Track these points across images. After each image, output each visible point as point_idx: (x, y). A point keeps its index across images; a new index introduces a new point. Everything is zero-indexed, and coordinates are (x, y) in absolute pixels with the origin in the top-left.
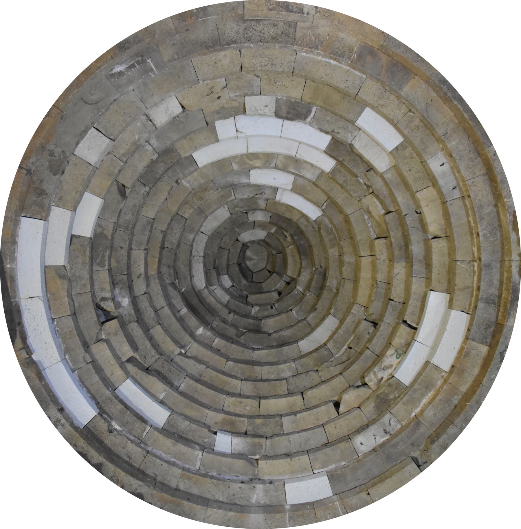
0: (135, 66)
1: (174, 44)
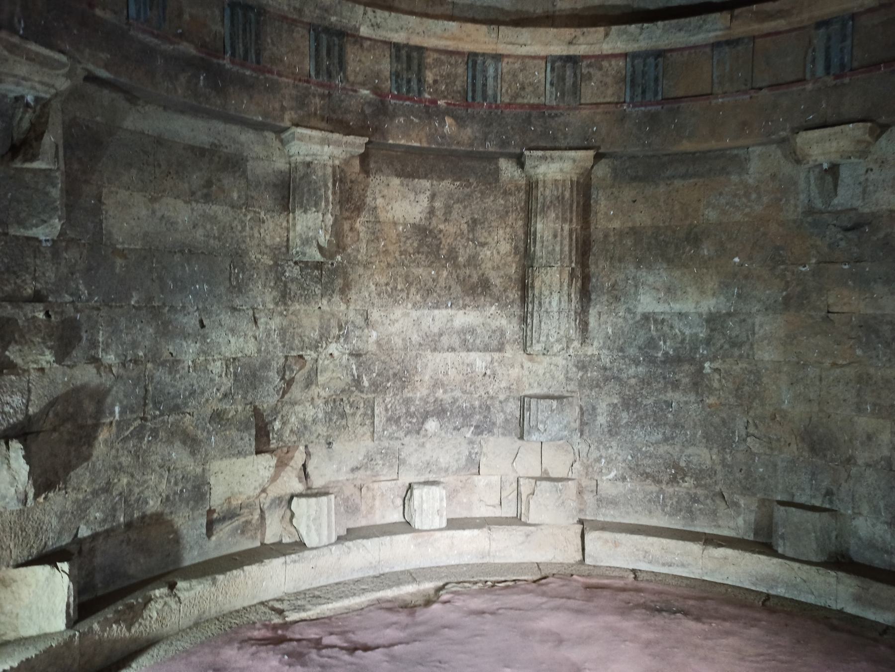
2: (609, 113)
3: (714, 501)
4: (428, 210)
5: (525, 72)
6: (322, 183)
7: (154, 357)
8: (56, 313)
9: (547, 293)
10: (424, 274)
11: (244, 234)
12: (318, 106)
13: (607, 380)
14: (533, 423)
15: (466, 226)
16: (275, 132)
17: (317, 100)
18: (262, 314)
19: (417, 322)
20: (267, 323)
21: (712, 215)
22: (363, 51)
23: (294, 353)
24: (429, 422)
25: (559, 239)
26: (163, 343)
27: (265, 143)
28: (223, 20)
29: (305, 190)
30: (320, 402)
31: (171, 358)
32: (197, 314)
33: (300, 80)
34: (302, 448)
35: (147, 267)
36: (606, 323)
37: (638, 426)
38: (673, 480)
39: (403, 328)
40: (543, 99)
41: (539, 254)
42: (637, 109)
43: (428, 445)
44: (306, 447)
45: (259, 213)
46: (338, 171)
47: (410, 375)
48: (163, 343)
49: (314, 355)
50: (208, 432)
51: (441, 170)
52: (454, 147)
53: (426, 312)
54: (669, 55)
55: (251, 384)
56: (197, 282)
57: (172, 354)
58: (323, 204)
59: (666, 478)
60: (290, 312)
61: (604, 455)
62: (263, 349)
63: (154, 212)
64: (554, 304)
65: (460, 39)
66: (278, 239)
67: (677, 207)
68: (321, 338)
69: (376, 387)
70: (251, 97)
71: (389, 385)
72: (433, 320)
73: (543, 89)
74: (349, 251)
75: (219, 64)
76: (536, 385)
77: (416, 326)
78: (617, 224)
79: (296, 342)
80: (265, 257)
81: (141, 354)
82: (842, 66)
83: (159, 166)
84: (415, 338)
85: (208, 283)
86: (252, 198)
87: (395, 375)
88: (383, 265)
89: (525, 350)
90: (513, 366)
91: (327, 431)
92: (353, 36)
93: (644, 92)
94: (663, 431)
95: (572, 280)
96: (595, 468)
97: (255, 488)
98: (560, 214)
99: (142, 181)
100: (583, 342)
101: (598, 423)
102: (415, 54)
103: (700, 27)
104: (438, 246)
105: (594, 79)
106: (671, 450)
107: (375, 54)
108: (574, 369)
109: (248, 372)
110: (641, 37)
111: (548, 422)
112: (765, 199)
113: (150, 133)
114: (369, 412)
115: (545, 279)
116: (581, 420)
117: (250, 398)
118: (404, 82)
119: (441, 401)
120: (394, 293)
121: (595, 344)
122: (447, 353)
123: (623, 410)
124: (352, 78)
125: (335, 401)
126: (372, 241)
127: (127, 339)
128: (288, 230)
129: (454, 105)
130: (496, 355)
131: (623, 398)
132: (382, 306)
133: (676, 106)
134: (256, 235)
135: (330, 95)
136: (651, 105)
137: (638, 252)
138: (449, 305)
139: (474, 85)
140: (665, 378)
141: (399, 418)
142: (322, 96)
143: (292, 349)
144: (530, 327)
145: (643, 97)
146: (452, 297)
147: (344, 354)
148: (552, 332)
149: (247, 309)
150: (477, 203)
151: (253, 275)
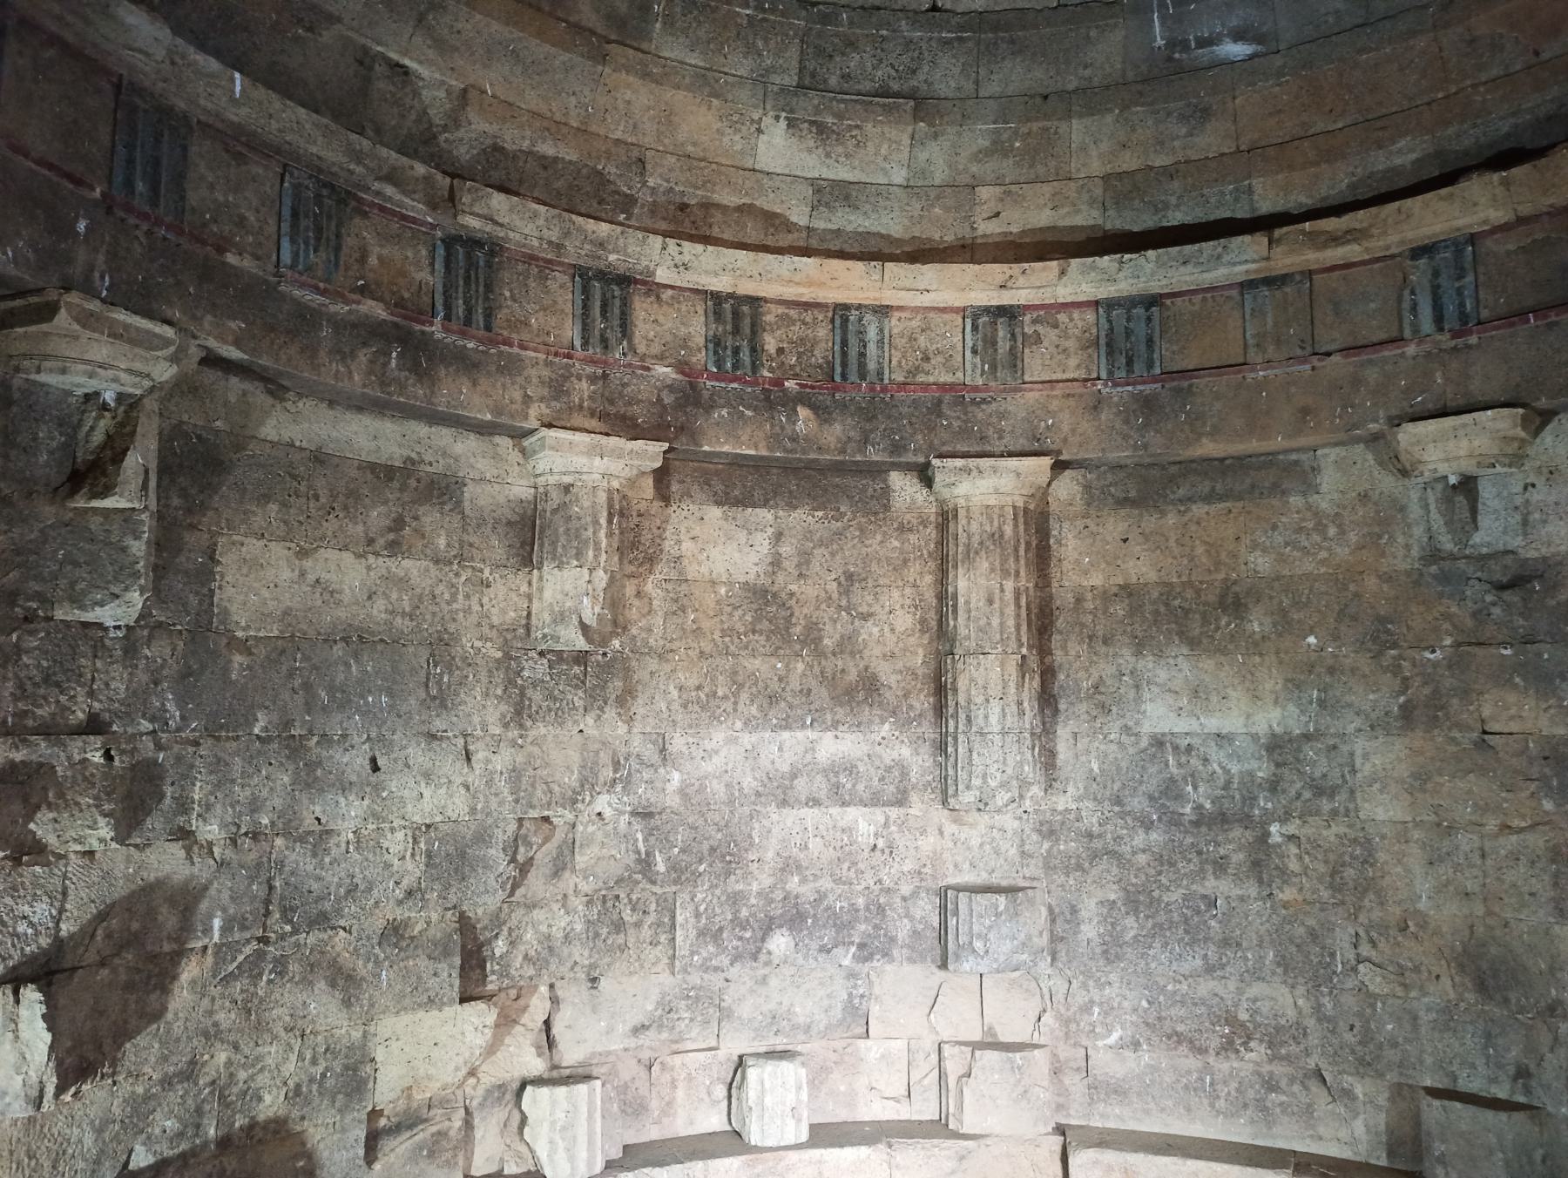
0: (1196, 38)
1: (1086, 67)
2: (1073, 396)
3: (1306, 1088)
4: (769, 560)
5: (928, 332)
6: (589, 519)
7: (288, 827)
8: (123, 752)
9: (979, 700)
10: (763, 669)
11: (455, 606)
12: (586, 394)
13: (1095, 856)
14: (963, 939)
15: (835, 584)
16: (512, 437)
17: (584, 384)
18: (480, 745)
19: (752, 754)
20: (488, 761)
21: (1262, 563)
22: (661, 306)
23: (534, 814)
24: (775, 937)
25: (996, 605)
26: (306, 801)
27: (496, 457)
28: (432, 264)
29: (561, 529)
30: (578, 903)
31: (317, 828)
32: (366, 746)
33: (556, 354)
34: (544, 989)
35: (284, 668)
36: (1088, 752)
37: (1157, 945)
38: (1228, 1047)
39: (726, 764)
40: (960, 375)
41: (962, 631)
42: (1119, 389)
43: (774, 982)
44: (552, 986)
45: (481, 571)
46: (616, 496)
47: (739, 850)
48: (306, 801)
49: (570, 816)
50: (377, 962)
51: (791, 492)
52: (812, 456)
53: (767, 734)
54: (1168, 302)
55: (456, 871)
56: (370, 692)
57: (318, 819)
58: (591, 553)
59: (1215, 1042)
60: (529, 740)
61: (1097, 999)
62: (479, 807)
63: (303, 574)
64: (994, 719)
65: (822, 284)
66: (512, 614)
67: (1200, 550)
68: (582, 786)
69: (681, 874)
70: (475, 384)
71: (701, 869)
72: (780, 749)
73: (960, 359)
74: (634, 631)
75: (423, 332)
76: (966, 866)
77: (750, 761)
78: (1096, 580)
79: (539, 793)
80: (489, 644)
81: (265, 821)
82: (1464, 317)
83: (316, 497)
84: (749, 782)
85: (390, 694)
86: (471, 545)
87: (713, 850)
88: (693, 654)
89: (945, 802)
90: (923, 832)
91: (590, 957)
92: (644, 283)
93: (1130, 362)
94: (1203, 952)
95: (1023, 677)
96: (1082, 1024)
97: (457, 1069)
98: (997, 563)
99: (285, 522)
100: (1048, 788)
101: (1082, 937)
102: (745, 309)
103: (1219, 257)
104: (788, 619)
105: (1045, 343)
106: (1221, 991)
107: (679, 310)
108: (1035, 837)
109: (451, 850)
110: (1121, 275)
111: (991, 936)
112: (1353, 537)
113: (304, 444)
114: (666, 920)
115: (975, 674)
116: (1052, 931)
117: (453, 899)
118: (729, 352)
119: (797, 897)
120: (712, 703)
121: (1071, 789)
122: (806, 809)
123: (1127, 913)
124: (641, 349)
125: (604, 899)
126: (674, 613)
127: (243, 794)
128: (529, 598)
129: (812, 387)
130: (894, 812)
131: (1125, 889)
132: (690, 726)
133: (1185, 384)
134: (476, 608)
135: (605, 376)
136: (1144, 383)
137: (1137, 626)
138: (808, 723)
139: (844, 354)
140: (1200, 853)
141: (721, 929)
142: (593, 379)
143: (532, 807)
144: (952, 759)
145: (1130, 370)
146: (812, 707)
147: (622, 813)
148: (993, 769)
149: (455, 736)
150: (854, 546)
151: (467, 677)
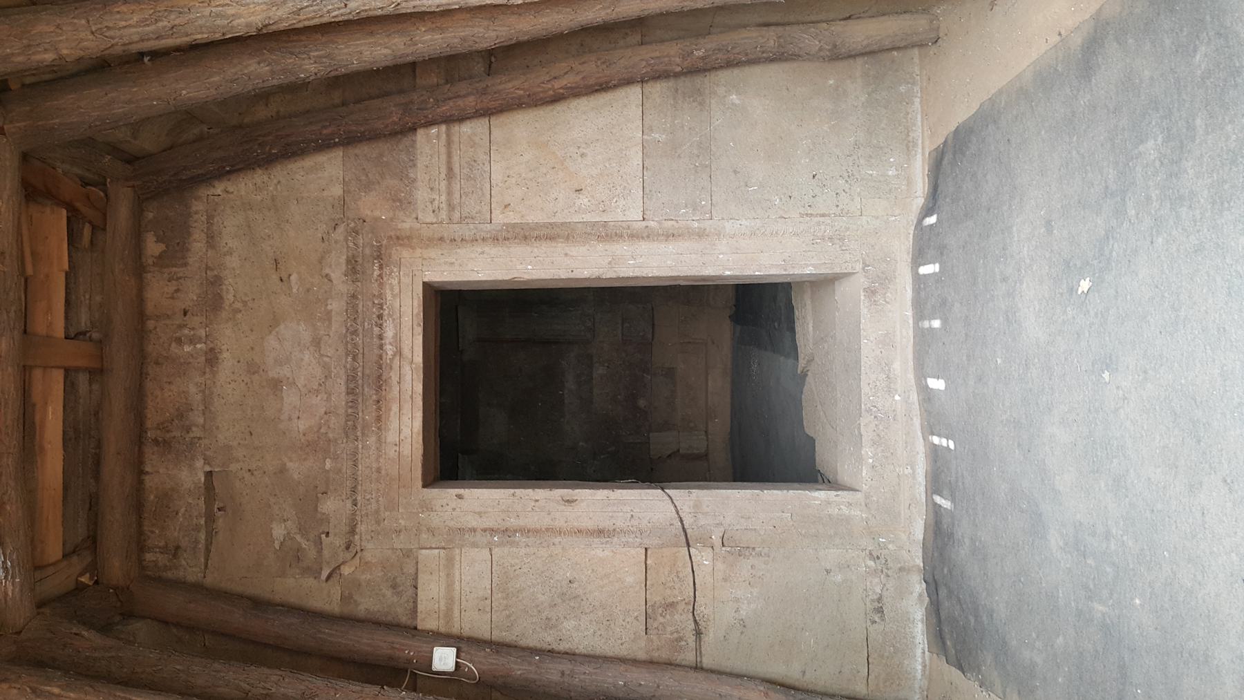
71: (614, 433)
